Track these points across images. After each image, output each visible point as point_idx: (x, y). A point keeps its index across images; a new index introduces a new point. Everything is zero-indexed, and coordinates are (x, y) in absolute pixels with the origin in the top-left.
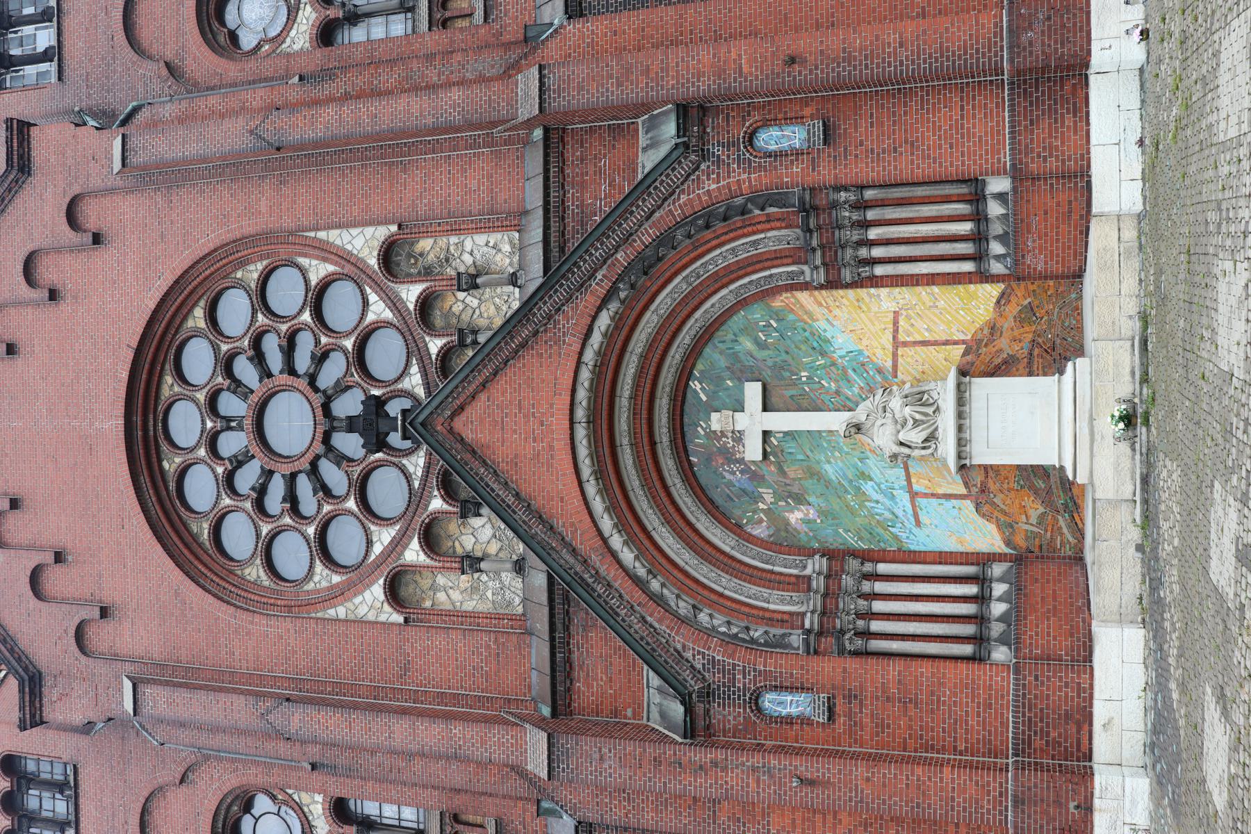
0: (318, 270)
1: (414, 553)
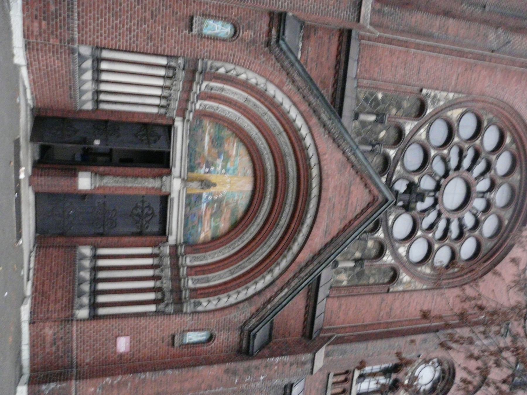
1: (408, 127)
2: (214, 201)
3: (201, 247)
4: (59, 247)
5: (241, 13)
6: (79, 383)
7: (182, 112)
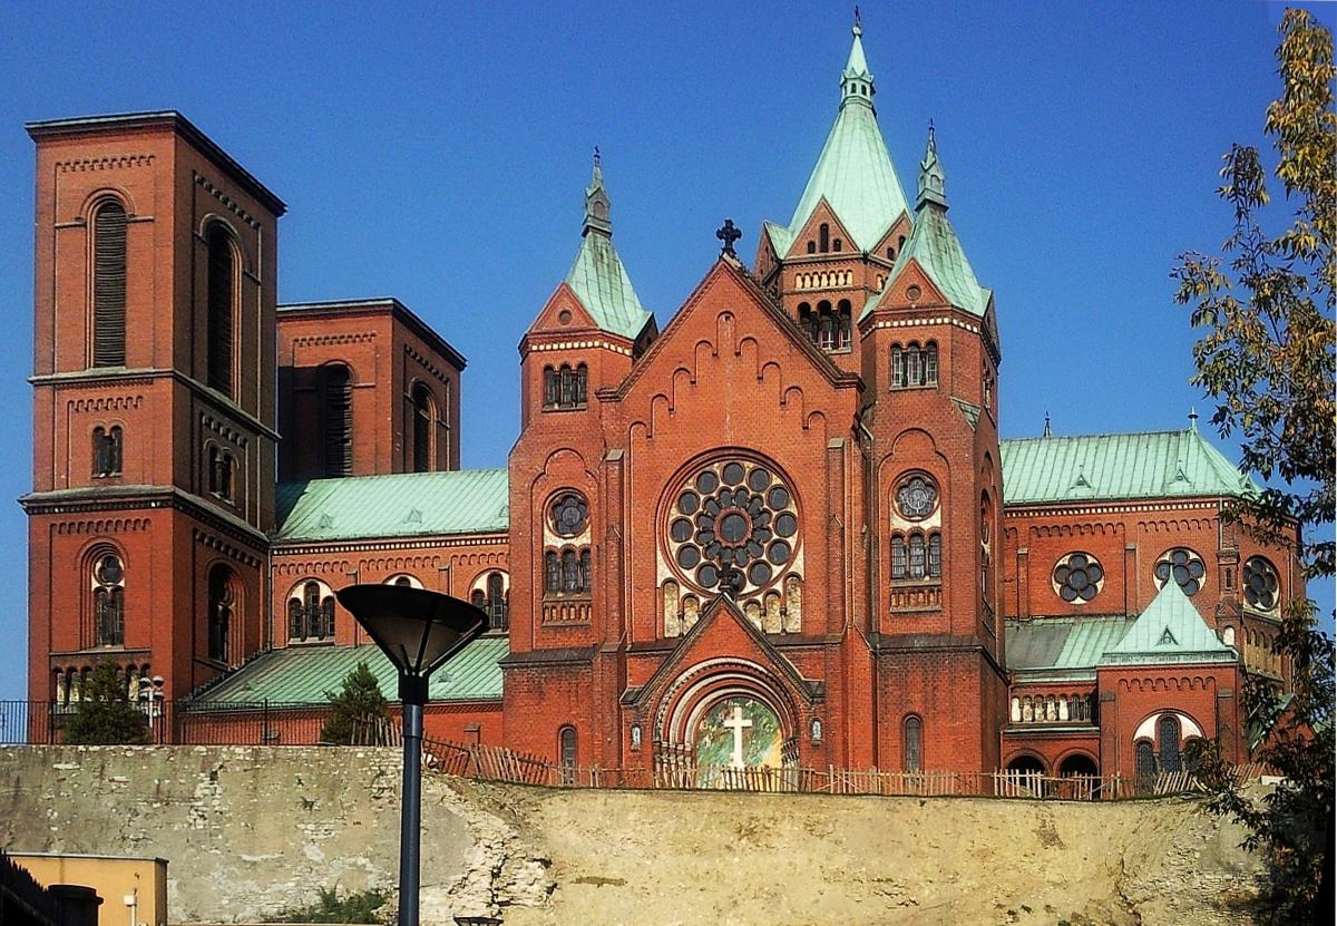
0: (792, 541)
1: (684, 591)
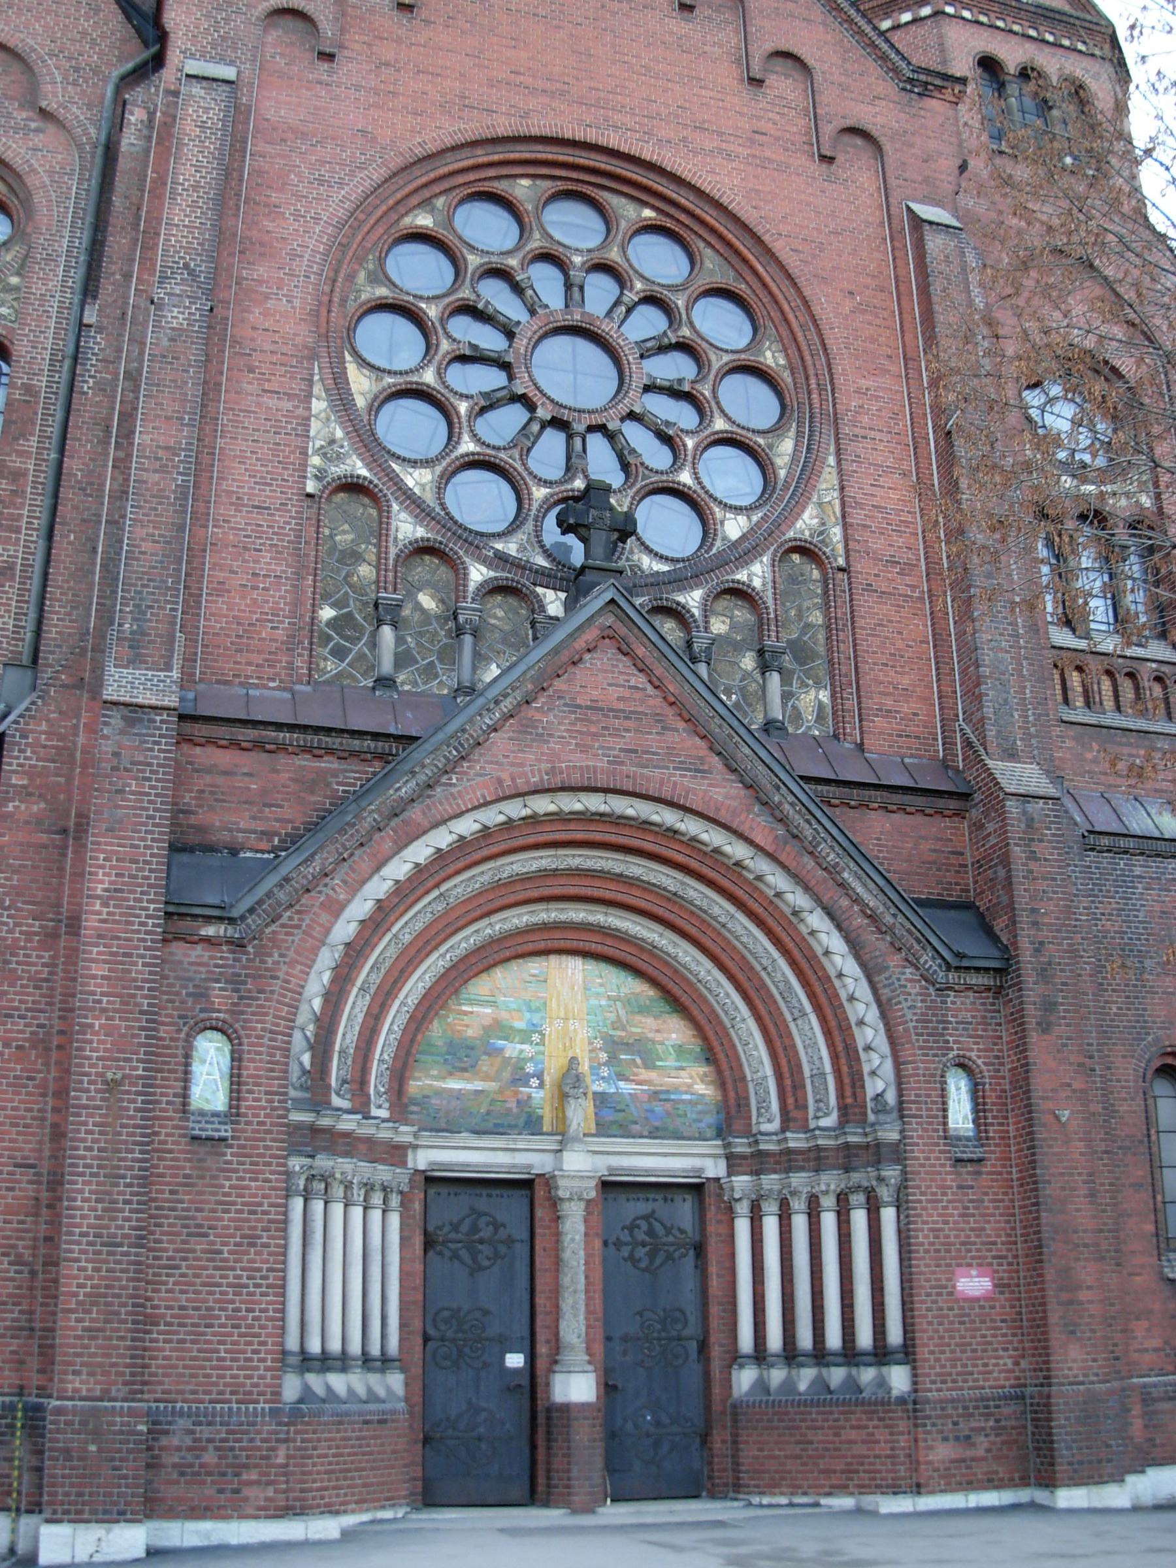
2: (613, 1060)
3: (732, 1094)
4: (735, 1442)
5: (171, 1016)
6: (1057, 1377)
7: (396, 1153)
